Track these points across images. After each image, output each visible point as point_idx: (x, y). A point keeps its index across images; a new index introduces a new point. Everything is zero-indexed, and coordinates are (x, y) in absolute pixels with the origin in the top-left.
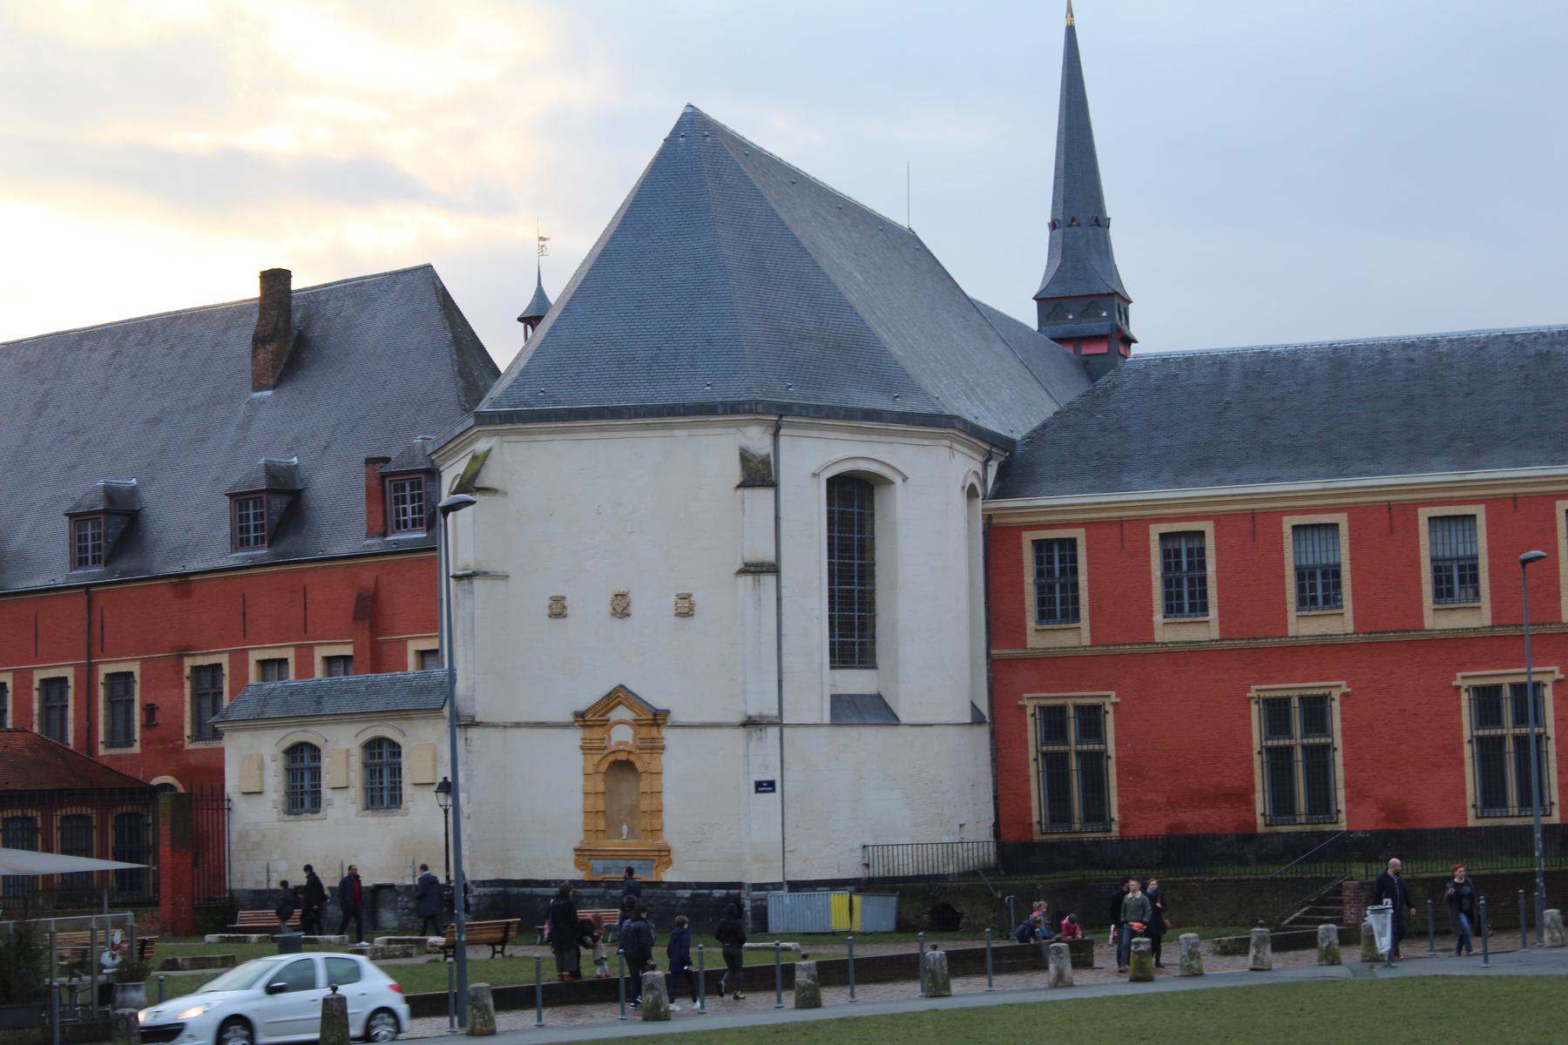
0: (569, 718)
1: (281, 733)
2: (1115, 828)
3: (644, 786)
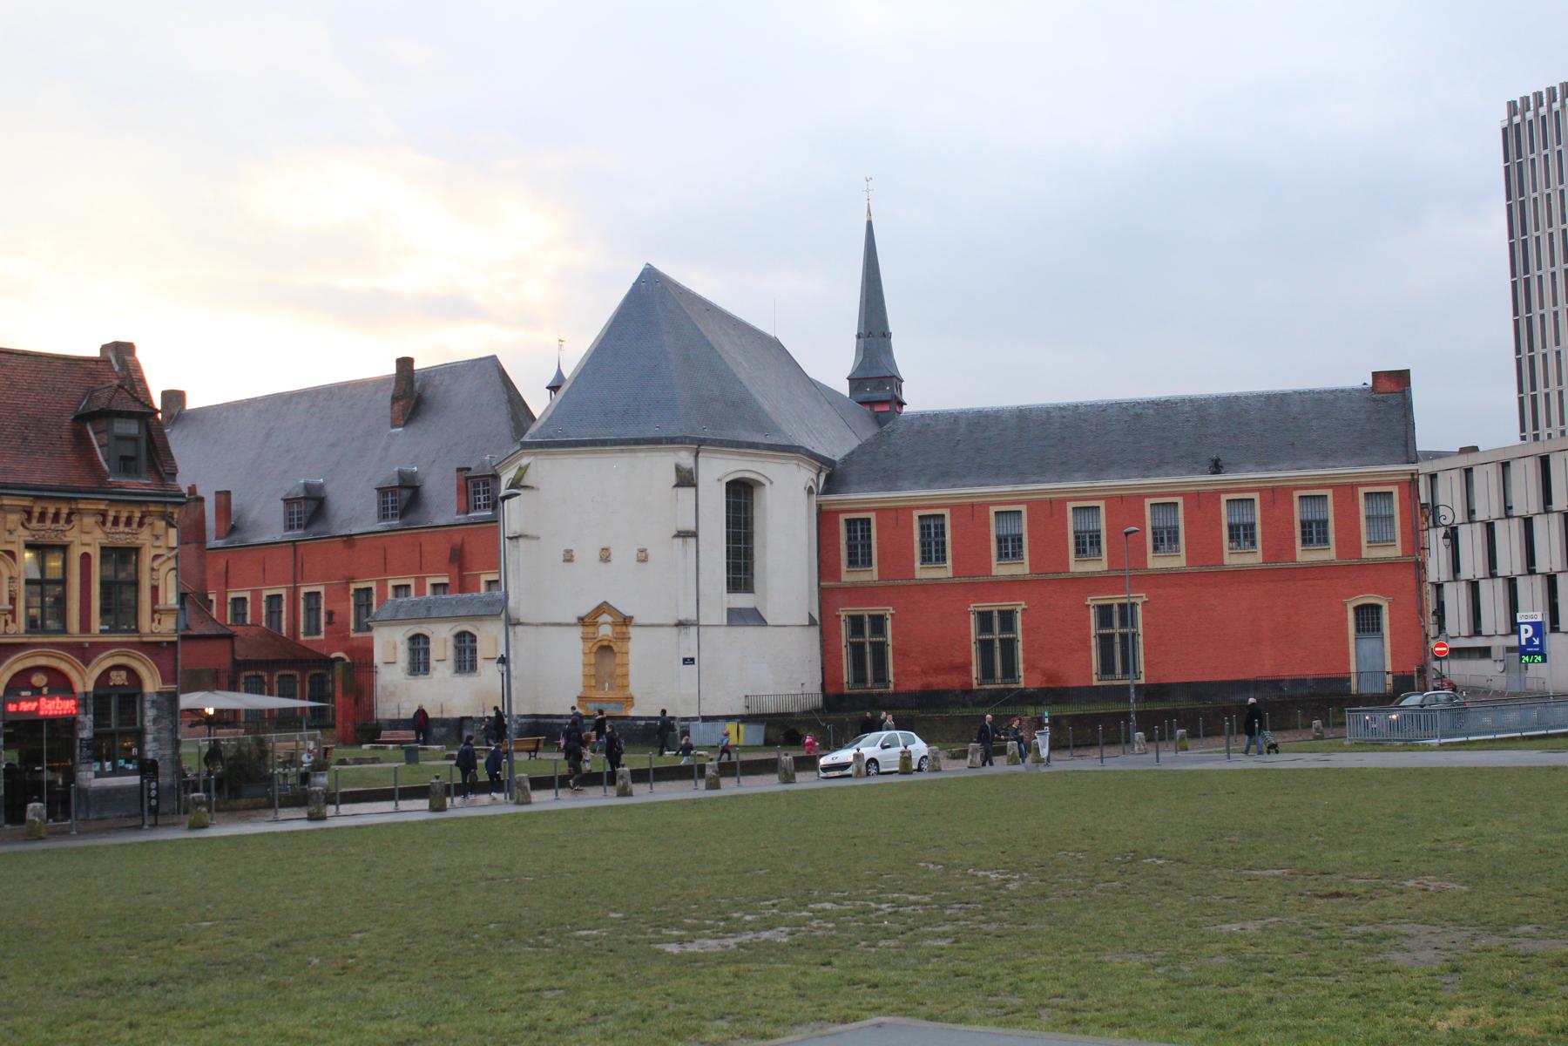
0: (574, 620)
1: (408, 627)
2: (891, 686)
3: (618, 660)
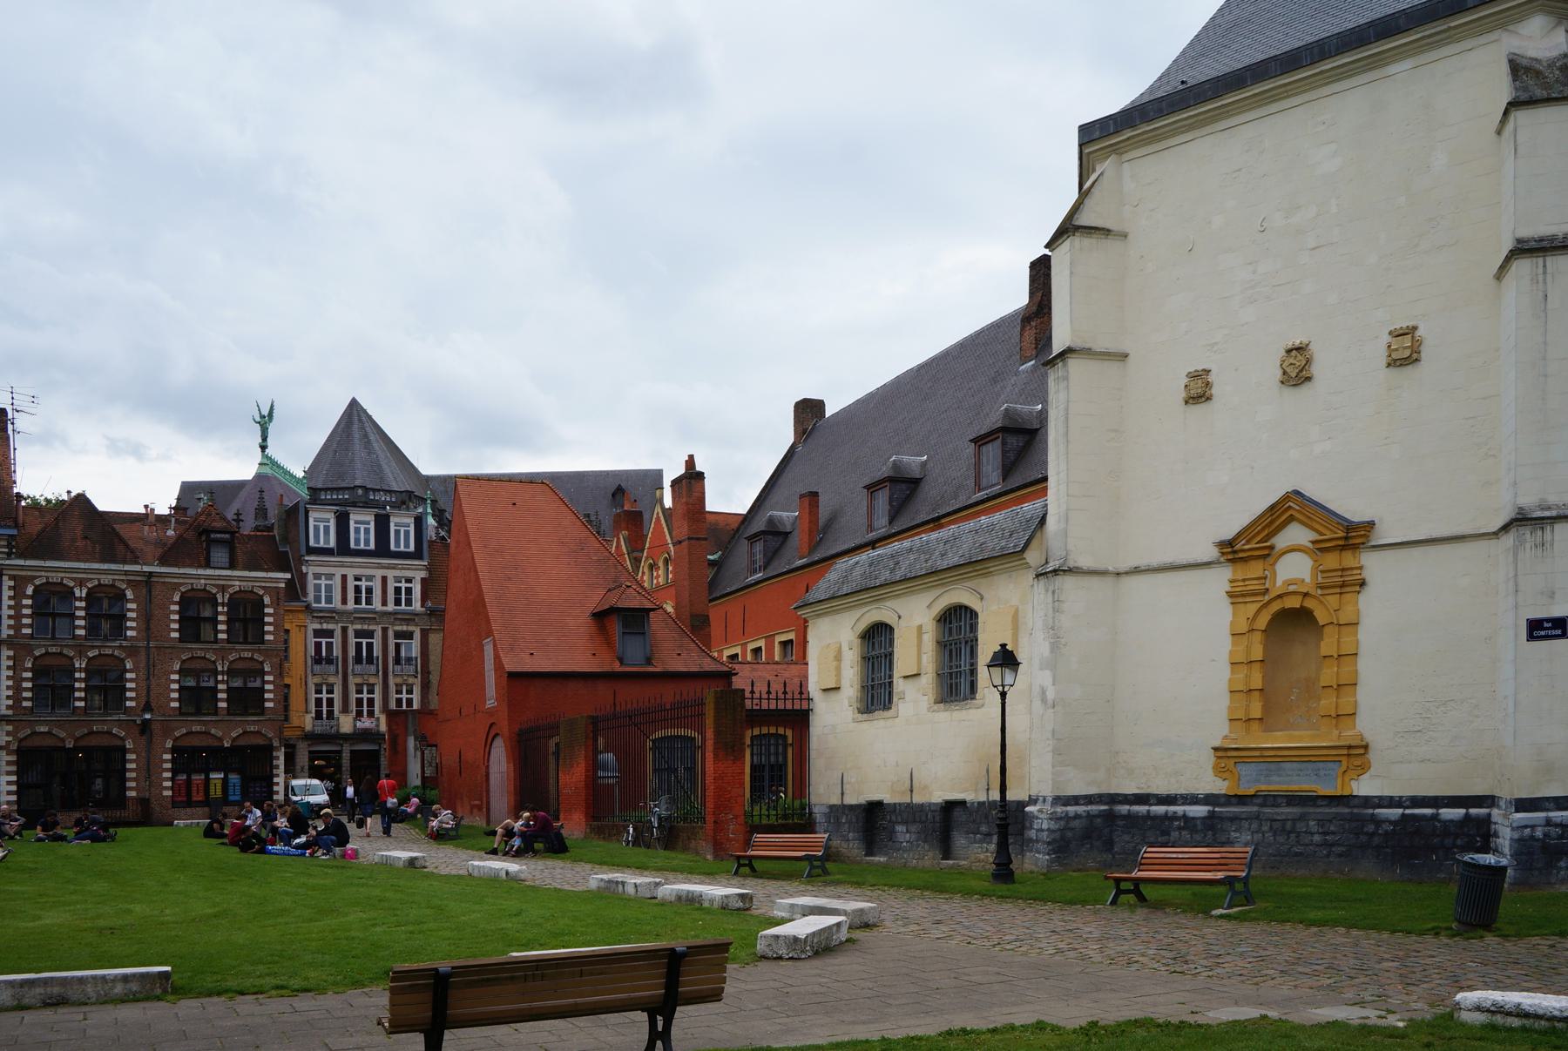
0: (1212, 553)
1: (856, 614)
3: (1327, 646)
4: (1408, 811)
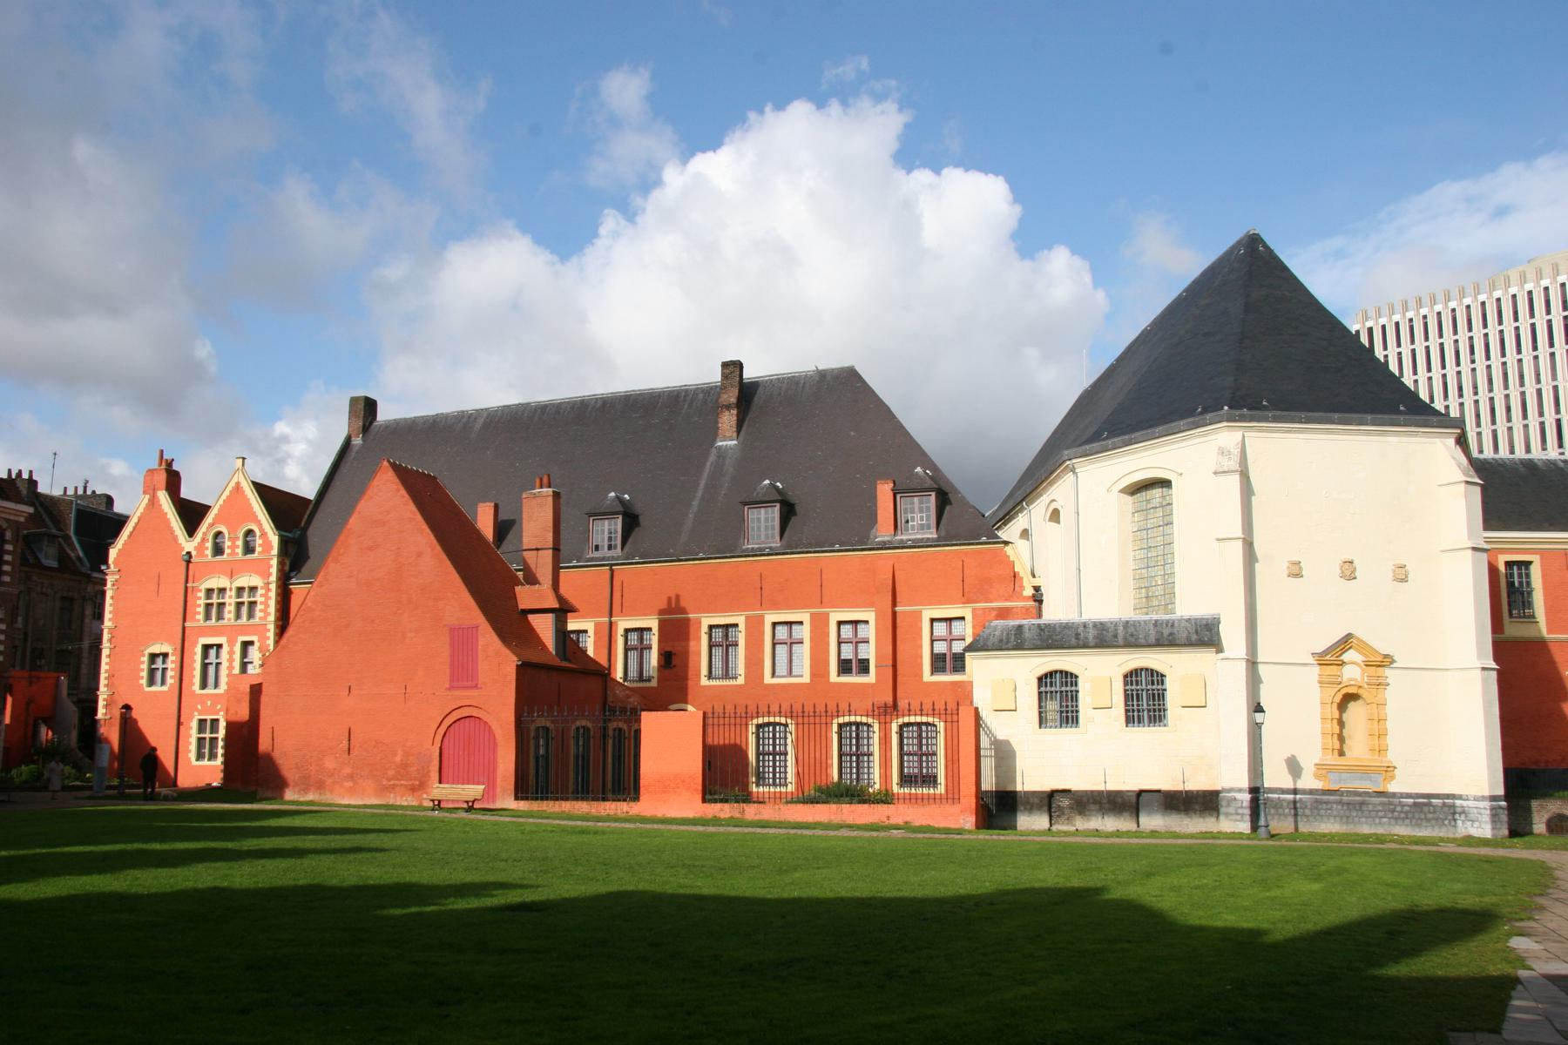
4: (1417, 800)
